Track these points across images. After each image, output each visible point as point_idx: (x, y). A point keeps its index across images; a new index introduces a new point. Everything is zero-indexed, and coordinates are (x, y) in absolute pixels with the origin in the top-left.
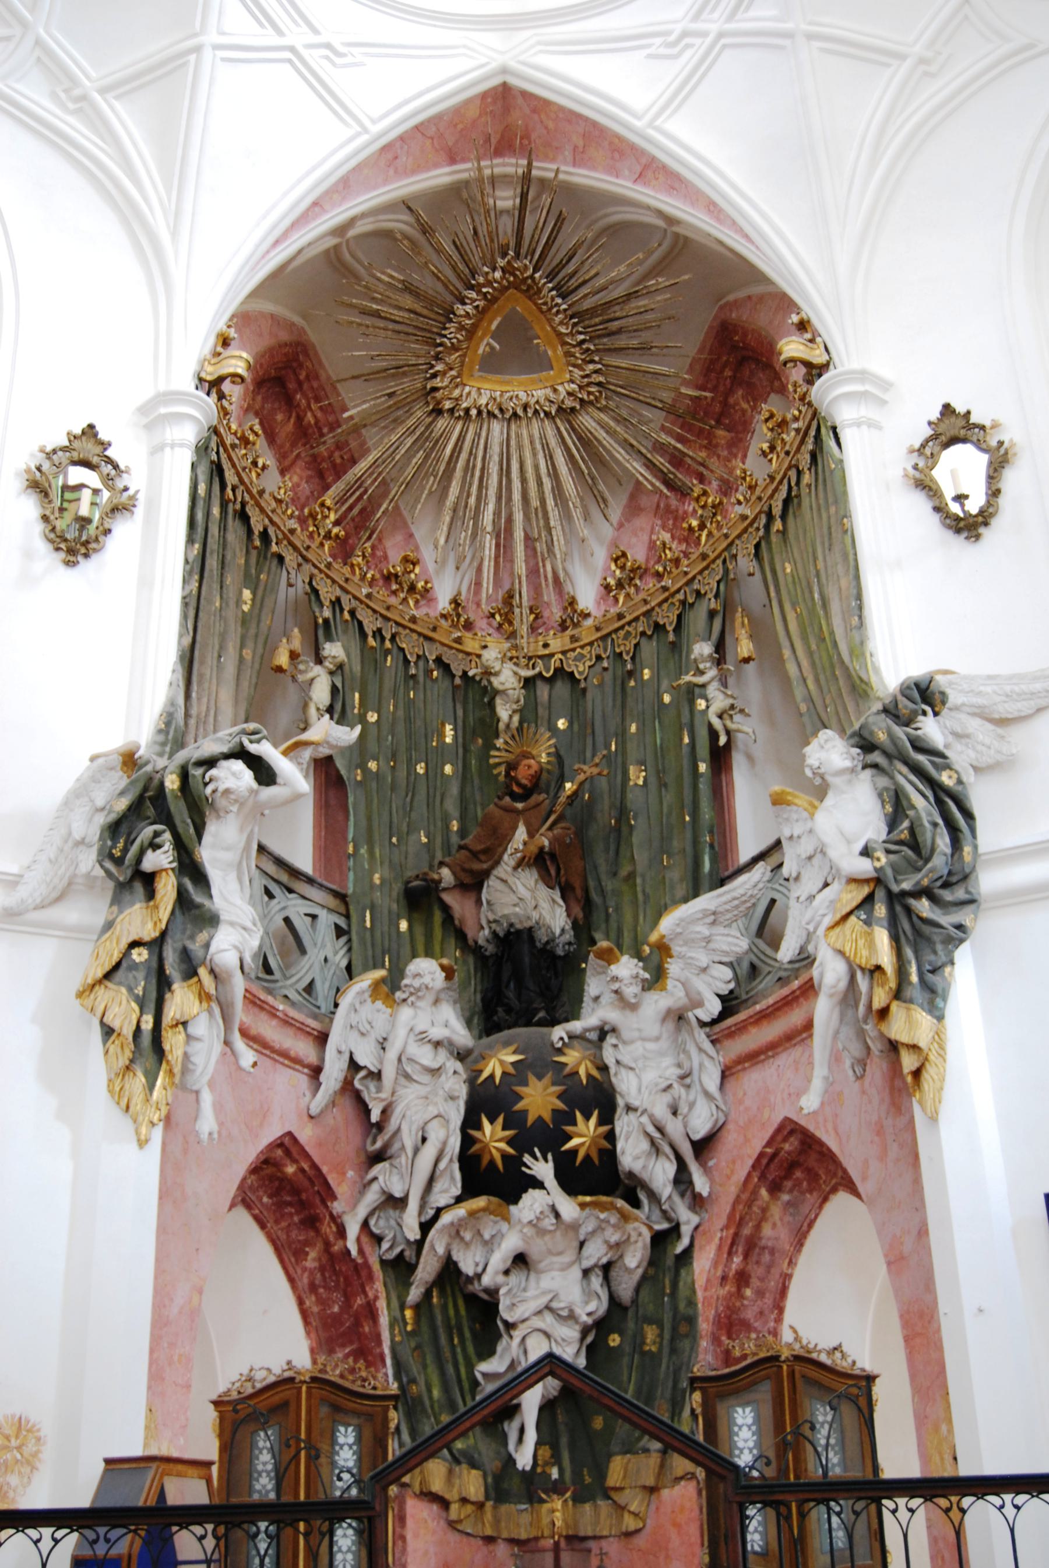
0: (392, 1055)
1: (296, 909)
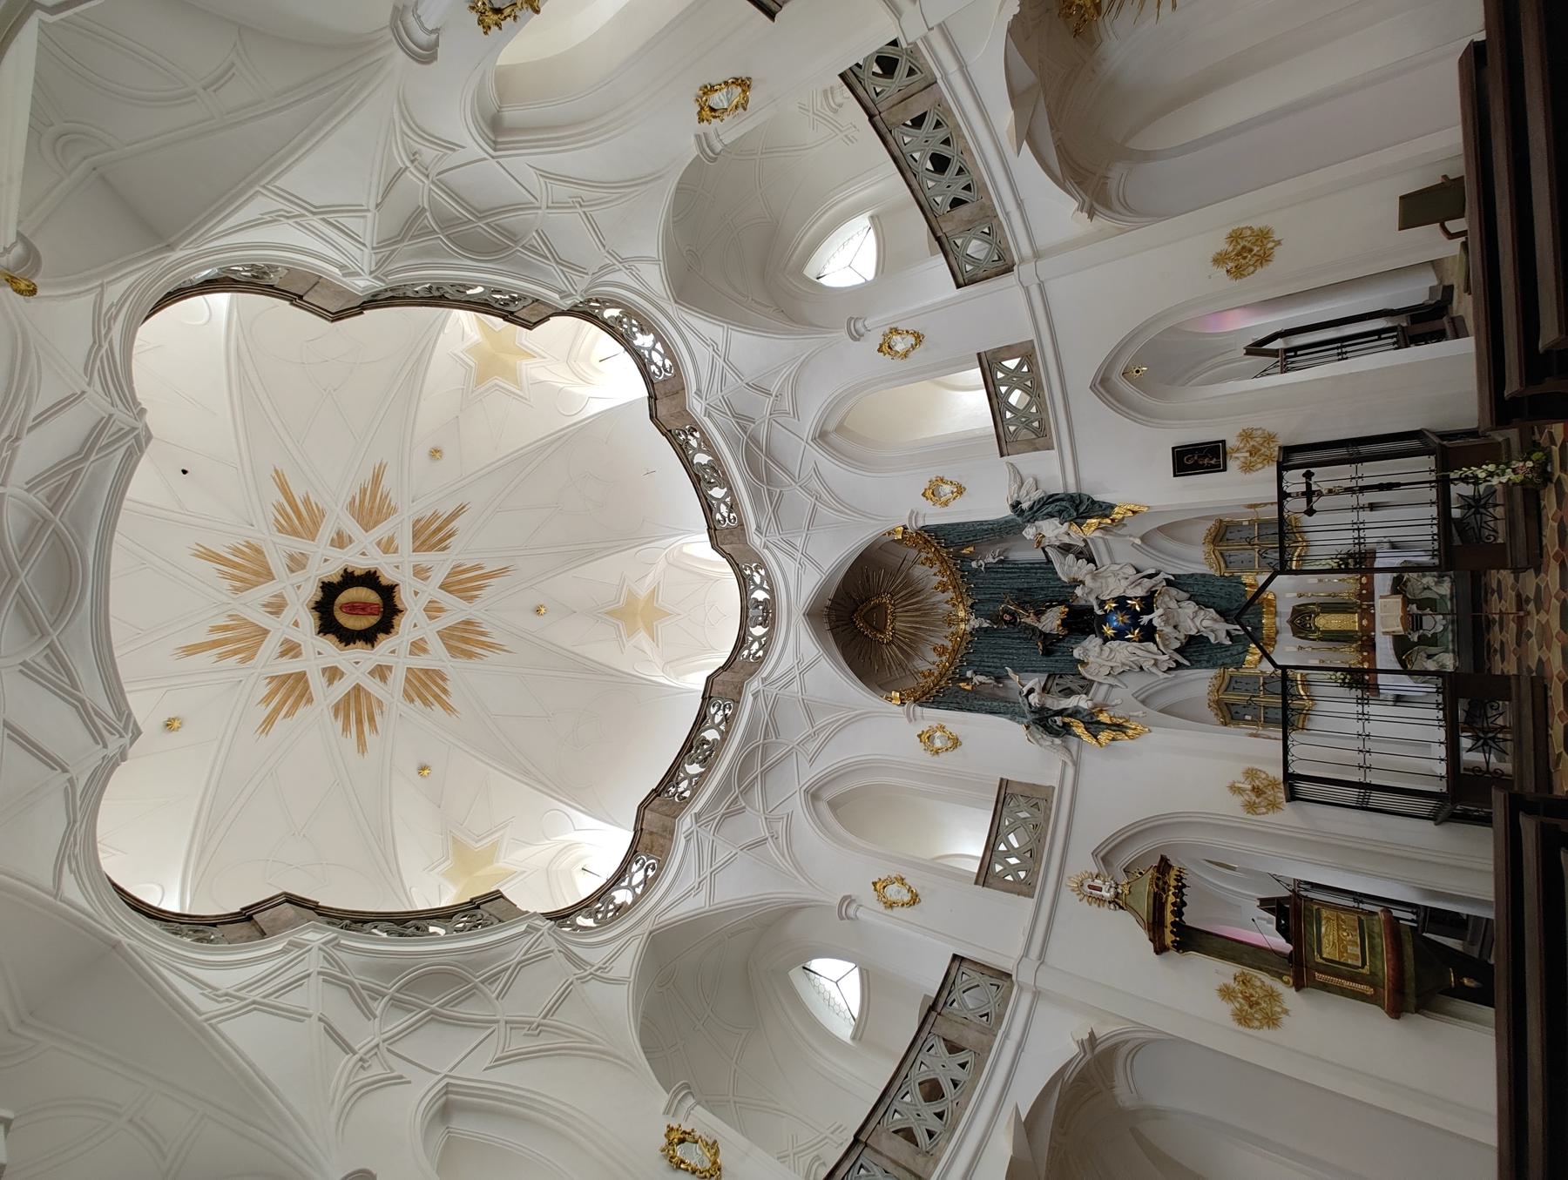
0: (1106, 663)
1: (1055, 689)
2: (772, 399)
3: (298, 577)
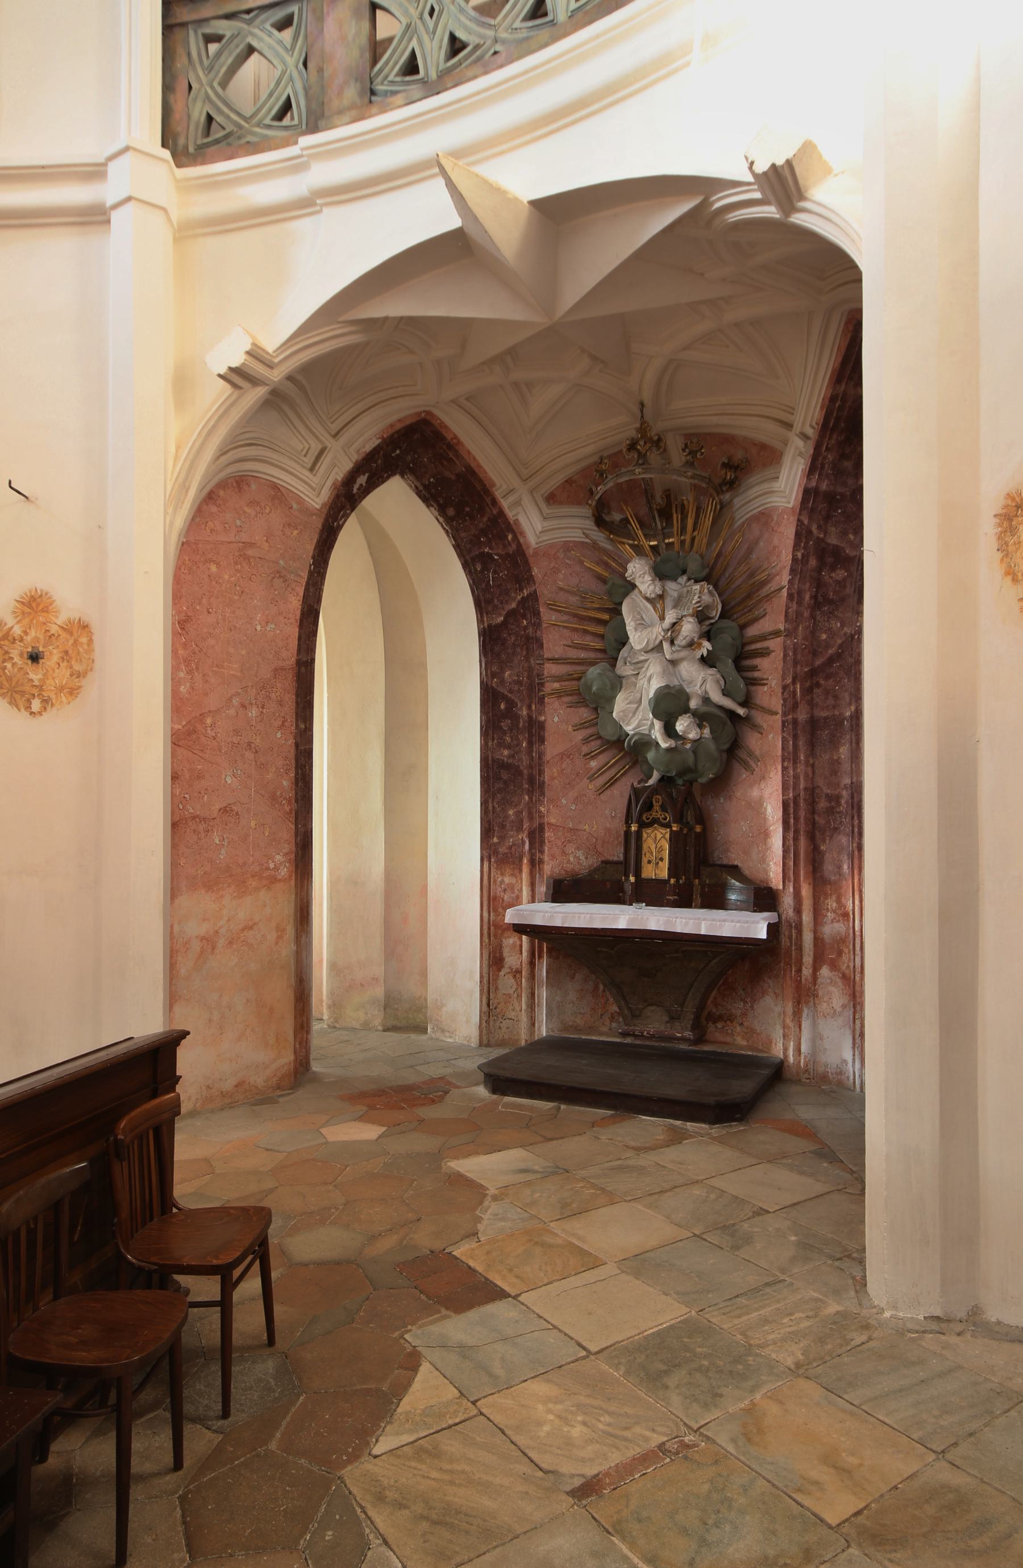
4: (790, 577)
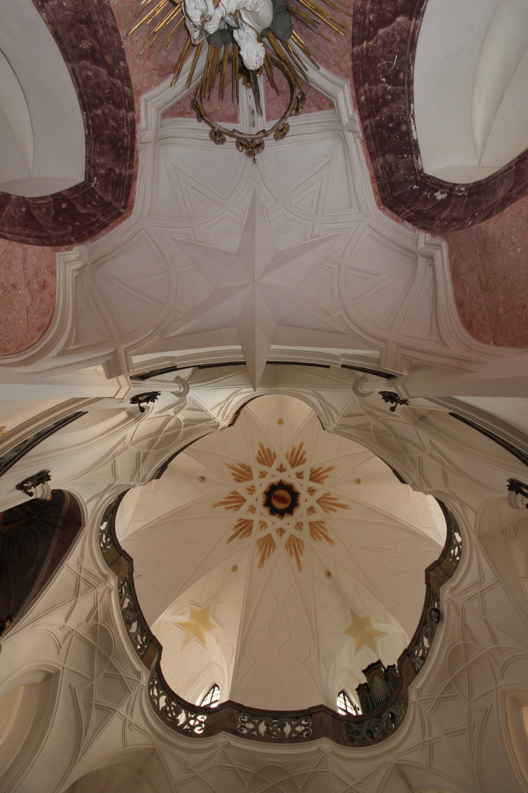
2: (94, 701)
3: (300, 520)
4: (123, 47)
